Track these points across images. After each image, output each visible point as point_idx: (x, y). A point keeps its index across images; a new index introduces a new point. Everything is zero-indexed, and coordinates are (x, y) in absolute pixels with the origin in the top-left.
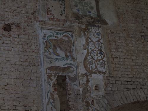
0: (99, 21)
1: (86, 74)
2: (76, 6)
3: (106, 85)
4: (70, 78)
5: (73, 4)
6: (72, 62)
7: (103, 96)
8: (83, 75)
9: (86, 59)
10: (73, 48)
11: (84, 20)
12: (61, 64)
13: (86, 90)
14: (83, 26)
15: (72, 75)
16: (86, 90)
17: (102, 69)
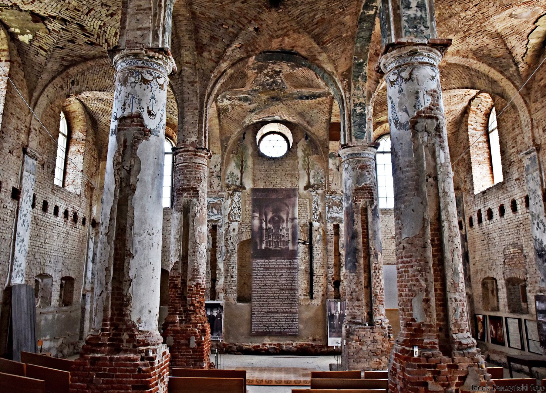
0: (242, 187)
1: (228, 223)
2: (228, 179)
3: (239, 228)
4: (218, 226)
5: (227, 177)
6: (220, 216)
7: (236, 235)
8: (227, 223)
9: (229, 213)
10: (223, 208)
11: (232, 188)
12: (214, 218)
13: (227, 231)
14: (231, 192)
15: (219, 224)
16: (227, 231)
17: (238, 219)
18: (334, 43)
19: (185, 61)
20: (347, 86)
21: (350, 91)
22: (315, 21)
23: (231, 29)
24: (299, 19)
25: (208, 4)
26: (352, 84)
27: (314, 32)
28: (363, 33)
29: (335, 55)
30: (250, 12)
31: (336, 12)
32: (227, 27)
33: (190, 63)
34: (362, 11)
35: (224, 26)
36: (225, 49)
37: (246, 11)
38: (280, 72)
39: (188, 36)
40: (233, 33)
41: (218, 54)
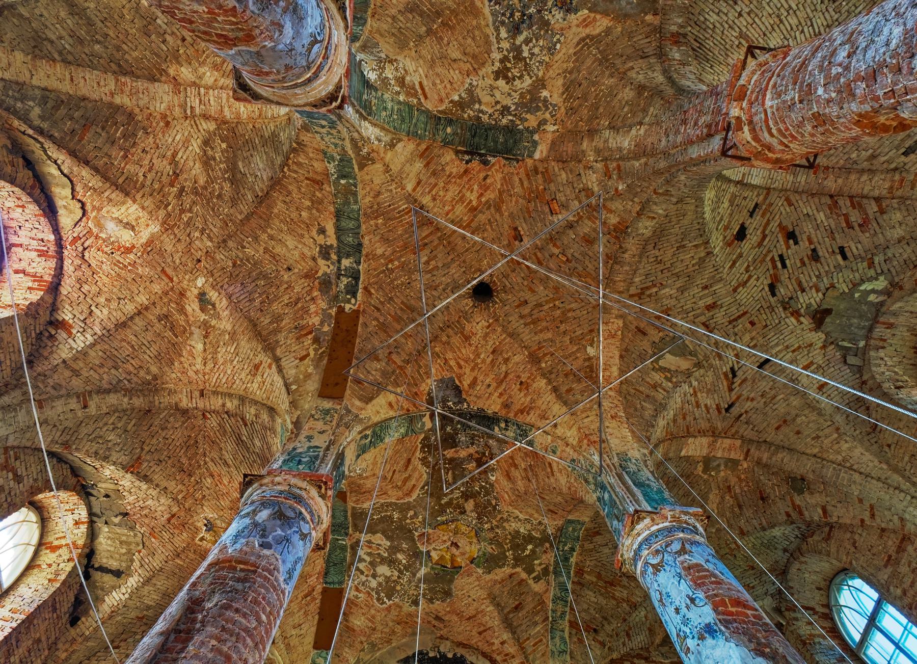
18: (395, 209)
19: (655, 221)
20: (360, 144)
21: (352, 140)
22: (427, 251)
23: (556, 251)
24: (450, 258)
25: (573, 306)
26: (350, 152)
27: (430, 231)
28: (351, 226)
29: (391, 190)
30: (520, 280)
31: (396, 263)
32: (560, 256)
33: (649, 217)
34: (361, 267)
35: (564, 259)
36: (577, 222)
37: (526, 283)
38: (498, 75)
39: (626, 256)
40: (555, 245)
41: (593, 216)
